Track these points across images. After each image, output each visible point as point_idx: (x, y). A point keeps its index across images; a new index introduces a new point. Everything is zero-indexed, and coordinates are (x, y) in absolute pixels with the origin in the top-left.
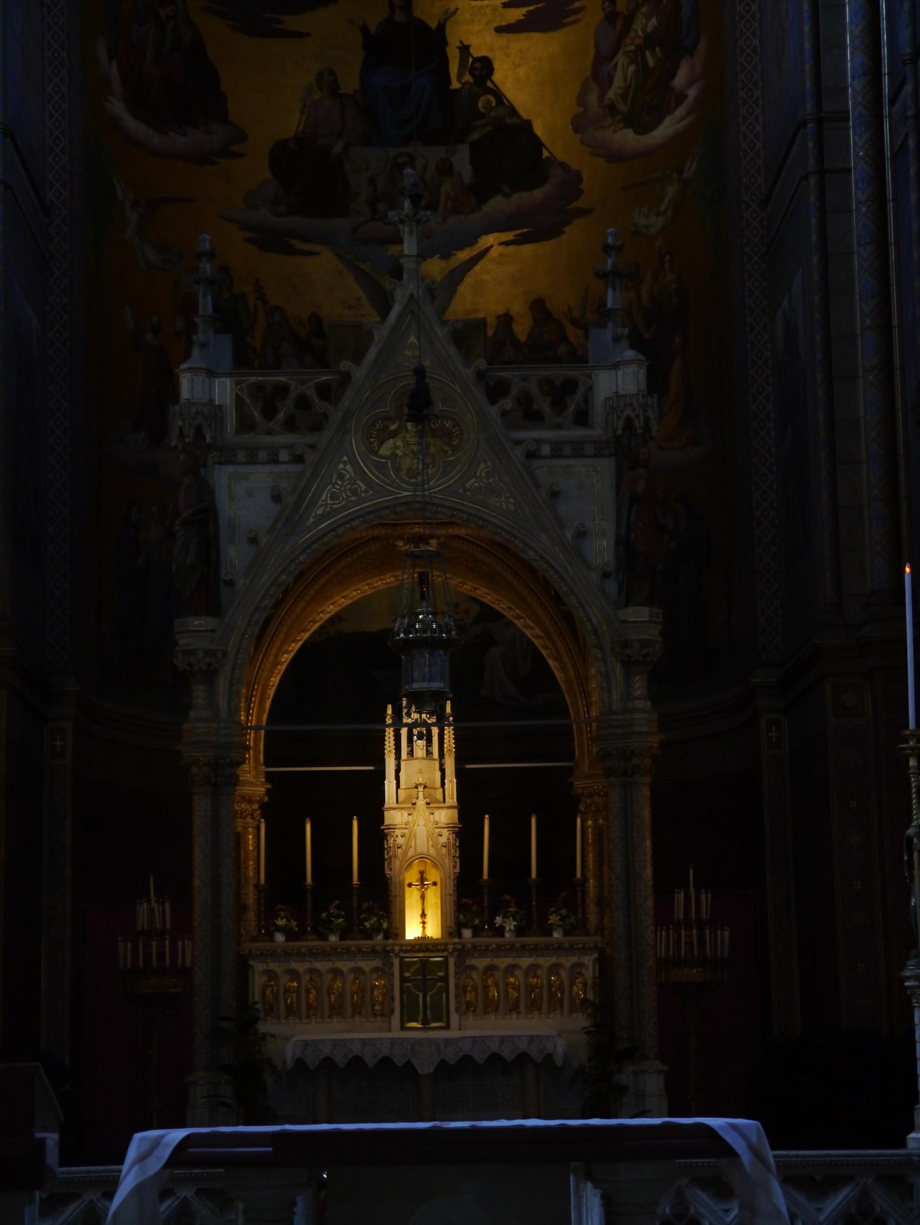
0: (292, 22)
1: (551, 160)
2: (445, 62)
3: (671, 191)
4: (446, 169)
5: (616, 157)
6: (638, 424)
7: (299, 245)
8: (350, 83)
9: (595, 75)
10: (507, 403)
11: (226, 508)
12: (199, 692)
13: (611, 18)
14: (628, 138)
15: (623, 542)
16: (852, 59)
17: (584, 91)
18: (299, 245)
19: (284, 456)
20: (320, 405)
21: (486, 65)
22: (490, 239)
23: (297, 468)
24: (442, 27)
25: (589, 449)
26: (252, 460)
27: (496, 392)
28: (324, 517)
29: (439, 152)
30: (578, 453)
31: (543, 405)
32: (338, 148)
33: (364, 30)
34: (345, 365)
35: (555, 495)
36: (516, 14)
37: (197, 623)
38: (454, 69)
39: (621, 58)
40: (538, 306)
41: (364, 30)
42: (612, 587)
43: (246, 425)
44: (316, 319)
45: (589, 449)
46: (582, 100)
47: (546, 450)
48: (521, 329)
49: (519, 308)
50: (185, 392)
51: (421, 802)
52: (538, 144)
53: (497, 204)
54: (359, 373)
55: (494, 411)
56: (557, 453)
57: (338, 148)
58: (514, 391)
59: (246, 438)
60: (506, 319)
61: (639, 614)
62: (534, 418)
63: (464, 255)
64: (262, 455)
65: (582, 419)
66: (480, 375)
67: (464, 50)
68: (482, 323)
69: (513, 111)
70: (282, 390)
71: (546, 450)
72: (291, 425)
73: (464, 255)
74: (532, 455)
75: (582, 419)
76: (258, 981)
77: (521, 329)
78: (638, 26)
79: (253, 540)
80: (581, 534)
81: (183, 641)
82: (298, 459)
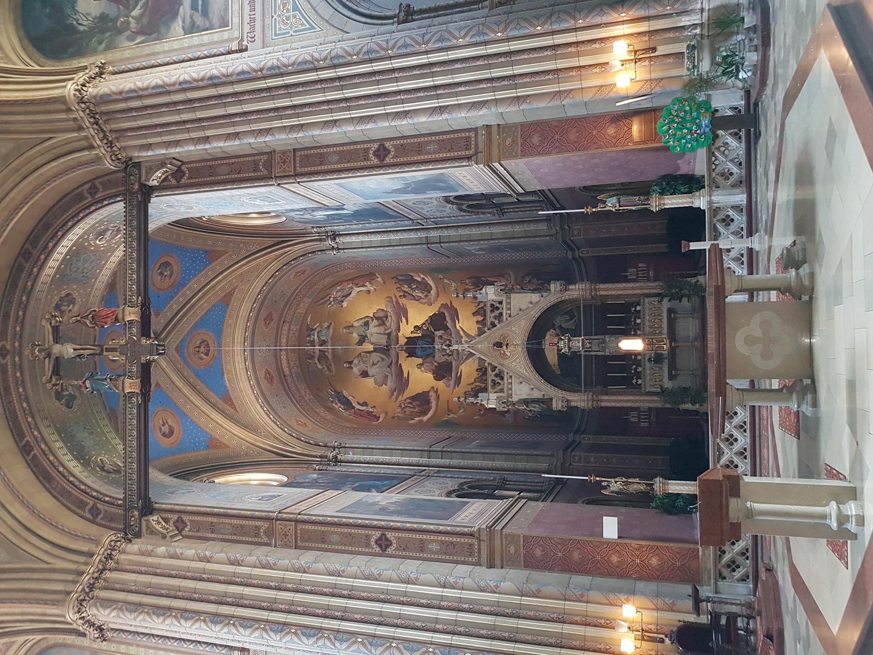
0: (405, 375)
1: (439, 311)
2: (415, 337)
3: (446, 281)
4: (441, 337)
5: (438, 295)
6: (502, 288)
7: (459, 374)
8: (420, 361)
9: (418, 300)
10: (496, 322)
11: (524, 396)
12: (573, 404)
13: (405, 296)
14: (433, 292)
15: (533, 291)
16: (413, 235)
17: (421, 303)
18: (459, 374)
19: (510, 381)
20: (497, 371)
21: (415, 327)
22: (458, 327)
23: (513, 377)
24: (407, 338)
25: (509, 301)
26: (511, 389)
27: (494, 325)
28: (526, 370)
29: (436, 339)
30: (510, 303)
31: (497, 313)
32: (436, 364)
33: (407, 357)
34: (486, 364)
35: (520, 310)
36: (404, 319)
37: (554, 405)
38: (416, 335)
39: (414, 294)
40: (474, 314)
41: (407, 357)
42: (545, 294)
43: (502, 391)
44: (477, 370)
45: (509, 301)
46: (424, 304)
47: (509, 312)
48: (481, 318)
49: (475, 319)
50: (494, 406)
51: (603, 345)
52: (435, 314)
53: (449, 325)
54: (488, 361)
55: (498, 326)
56: (510, 309)
57: (436, 364)
58: (493, 320)
59: (505, 390)
60: (477, 322)
61: (552, 286)
62: (501, 314)
63: (461, 333)
64: (510, 386)
65: (501, 303)
66: (489, 329)
67: (412, 332)
68: (479, 328)
69: (427, 320)
70: (493, 381)
71: (509, 312)
72: (502, 378)
73: (461, 333)
74: (510, 316)
75: (501, 303)
76: (653, 390)
77: (481, 318)
78: (406, 290)
79: (532, 389)
80: (531, 303)
81: (560, 408)
82: (511, 377)
